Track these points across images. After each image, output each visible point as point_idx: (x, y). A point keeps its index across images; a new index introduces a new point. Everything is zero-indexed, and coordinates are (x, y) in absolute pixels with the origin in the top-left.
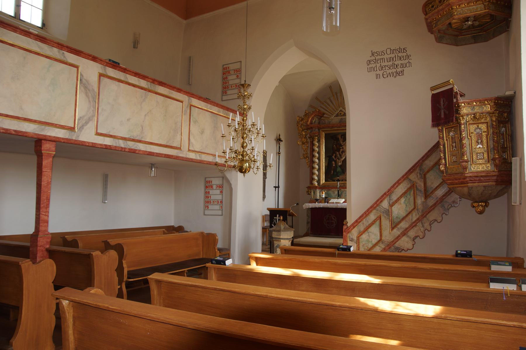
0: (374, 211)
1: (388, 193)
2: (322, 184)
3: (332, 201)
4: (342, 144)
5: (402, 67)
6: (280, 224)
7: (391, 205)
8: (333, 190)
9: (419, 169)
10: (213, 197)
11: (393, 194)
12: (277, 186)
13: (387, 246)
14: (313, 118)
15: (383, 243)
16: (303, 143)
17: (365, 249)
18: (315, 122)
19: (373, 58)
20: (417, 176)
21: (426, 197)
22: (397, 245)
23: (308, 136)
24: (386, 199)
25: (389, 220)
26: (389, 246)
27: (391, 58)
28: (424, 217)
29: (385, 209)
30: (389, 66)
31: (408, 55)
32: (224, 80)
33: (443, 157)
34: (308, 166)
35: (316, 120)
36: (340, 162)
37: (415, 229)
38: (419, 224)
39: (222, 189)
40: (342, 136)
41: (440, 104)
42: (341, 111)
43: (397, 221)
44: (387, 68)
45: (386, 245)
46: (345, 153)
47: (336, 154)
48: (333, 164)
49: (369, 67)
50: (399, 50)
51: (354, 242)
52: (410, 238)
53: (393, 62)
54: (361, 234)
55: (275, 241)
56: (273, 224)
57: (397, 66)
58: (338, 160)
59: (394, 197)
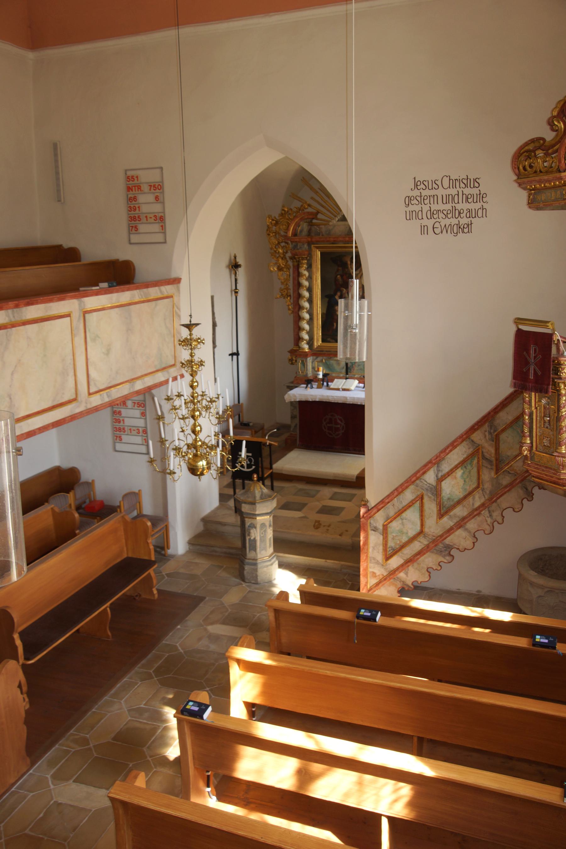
0: (412, 487)
1: (436, 461)
2: (317, 348)
3: (338, 383)
5: (470, 217)
6: (254, 489)
7: (440, 480)
9: (488, 426)
10: (128, 422)
11: (443, 462)
12: (235, 351)
13: (431, 542)
14: (298, 225)
15: (425, 537)
16: (280, 269)
17: (396, 544)
18: (301, 231)
19: (416, 193)
20: (485, 436)
21: (498, 470)
22: (448, 541)
23: (289, 255)
24: (432, 469)
25: (435, 502)
26: (436, 544)
27: (450, 196)
28: (493, 503)
29: (430, 484)
31: (482, 193)
32: (129, 203)
33: (528, 433)
34: (290, 312)
35: (304, 226)
37: (478, 519)
38: (485, 513)
39: (143, 409)
41: (528, 352)
43: (448, 504)
44: (441, 215)
45: (431, 540)
47: (341, 291)
49: (408, 209)
50: (465, 181)
51: (378, 532)
52: (470, 532)
53: (454, 205)
54: (390, 520)
55: (246, 518)
57: (460, 213)
59: (446, 467)
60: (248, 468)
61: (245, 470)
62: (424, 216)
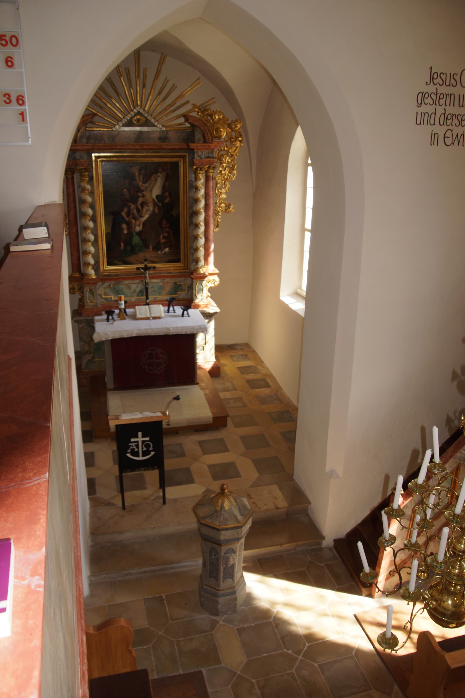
3: (142, 311)
4: (142, 188)
8: (126, 282)
18: (82, 137)
19: (431, 89)
30: (460, 118)
36: (139, 226)
40: (140, 170)
42: (139, 113)
46: (147, 206)
47: (129, 207)
48: (122, 229)
49: (420, 110)
56: (129, 453)
58: (133, 221)
60: (143, 456)
61: (141, 458)
62: (437, 122)
